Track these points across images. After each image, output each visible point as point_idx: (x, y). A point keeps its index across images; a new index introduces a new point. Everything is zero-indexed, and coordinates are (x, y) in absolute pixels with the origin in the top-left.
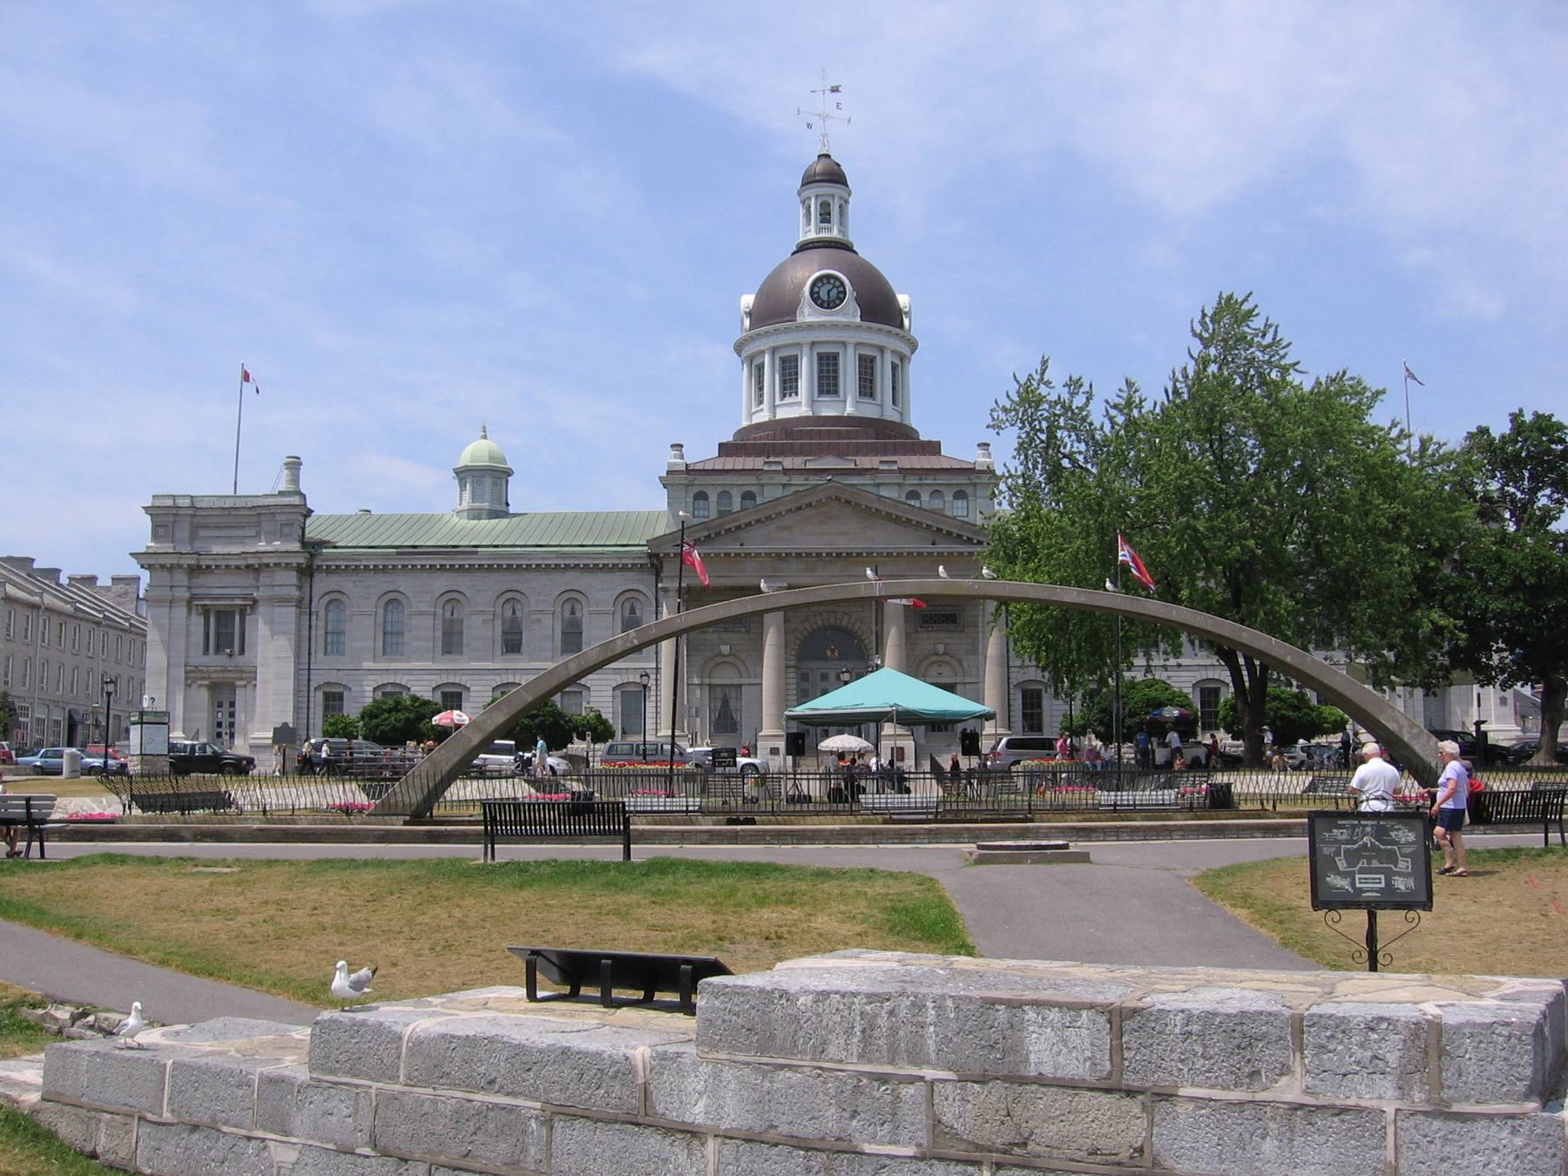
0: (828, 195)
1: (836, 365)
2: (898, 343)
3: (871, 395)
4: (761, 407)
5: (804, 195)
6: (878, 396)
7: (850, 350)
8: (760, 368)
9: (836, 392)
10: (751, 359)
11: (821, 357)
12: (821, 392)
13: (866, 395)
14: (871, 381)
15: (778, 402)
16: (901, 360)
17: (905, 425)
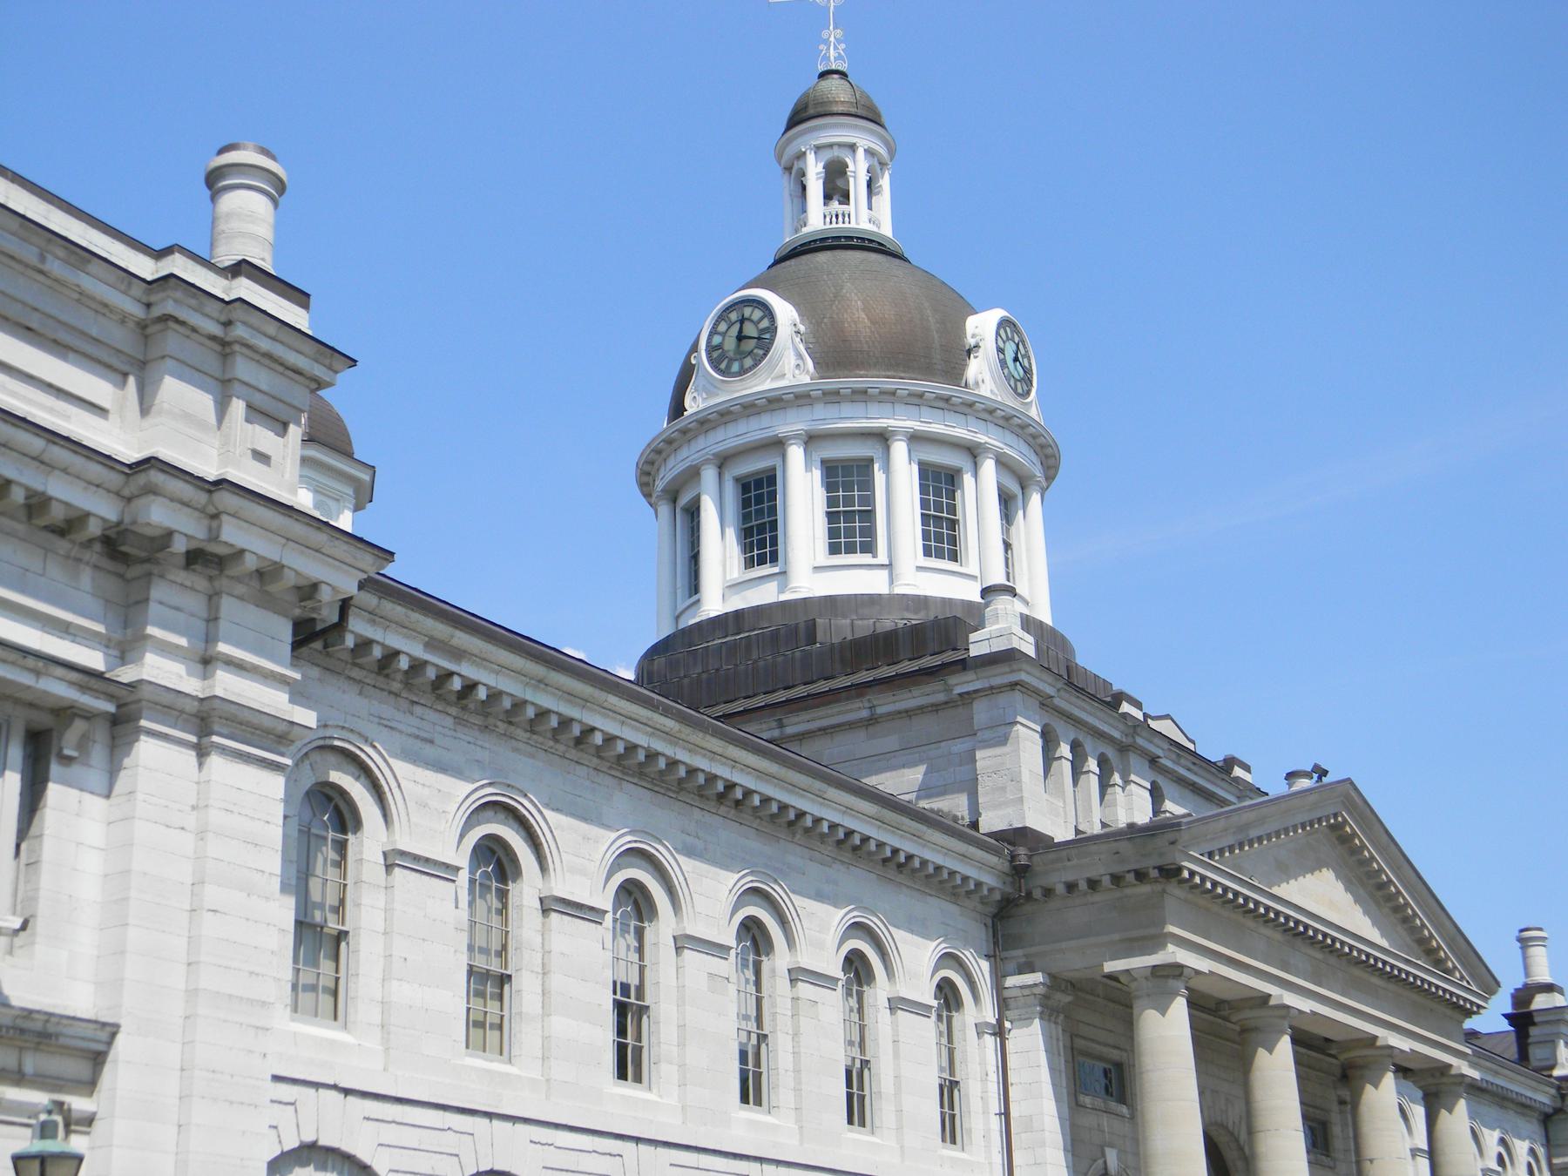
0: (840, 145)
4: (695, 598)
5: (790, 151)
8: (693, 512)
9: (869, 548)
10: (672, 495)
12: (834, 549)
13: (940, 555)
14: (953, 524)
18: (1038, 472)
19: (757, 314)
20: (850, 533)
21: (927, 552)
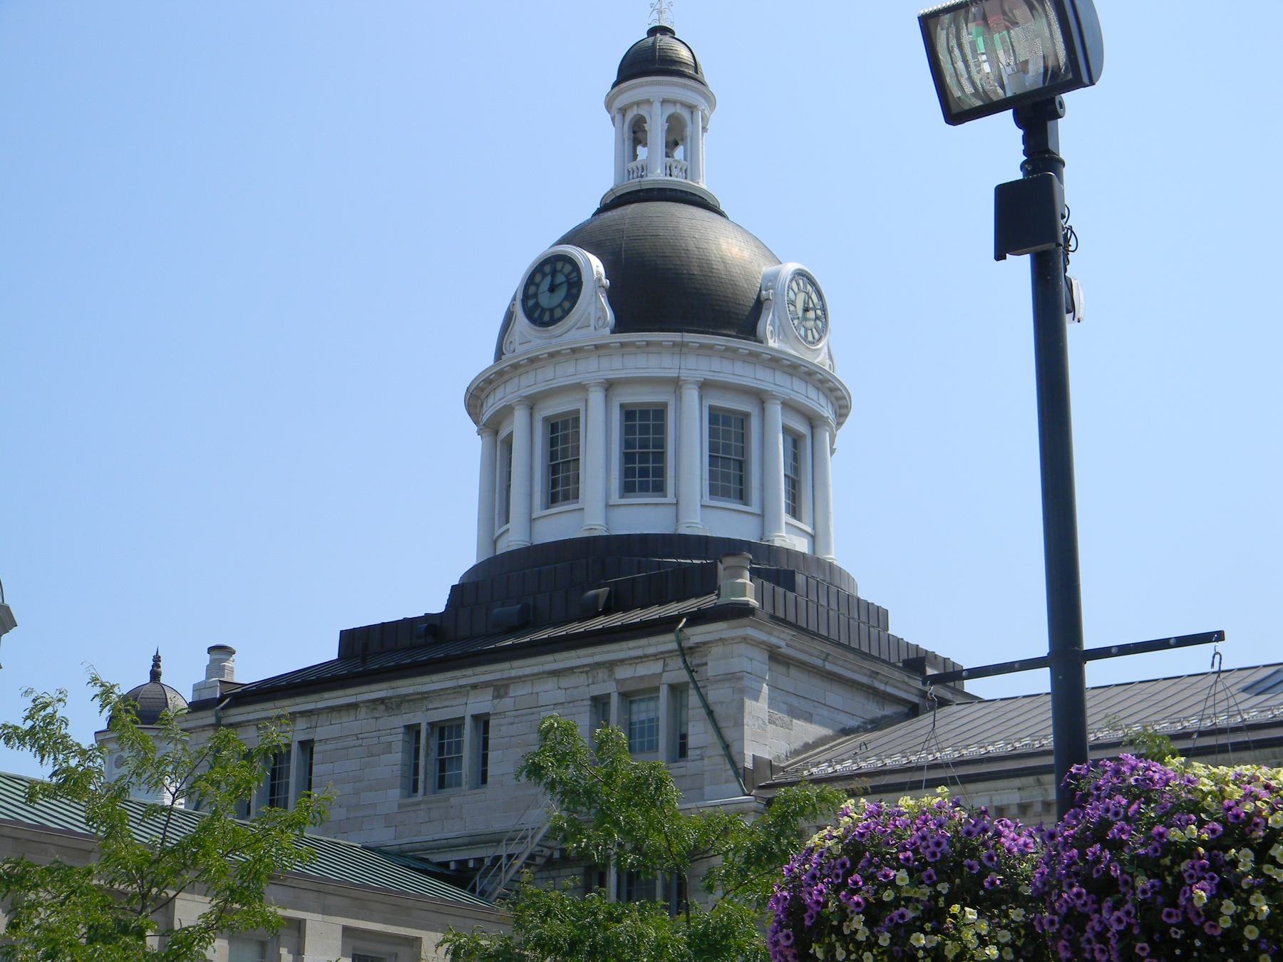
1: (661, 429)
2: (812, 393)
3: (742, 496)
6: (755, 494)
7: (691, 397)
9: (659, 488)
11: (629, 414)
12: (628, 488)
15: (538, 512)
16: (812, 427)
17: (821, 565)
18: (828, 412)
19: (568, 268)
20: (644, 473)
21: (713, 491)
